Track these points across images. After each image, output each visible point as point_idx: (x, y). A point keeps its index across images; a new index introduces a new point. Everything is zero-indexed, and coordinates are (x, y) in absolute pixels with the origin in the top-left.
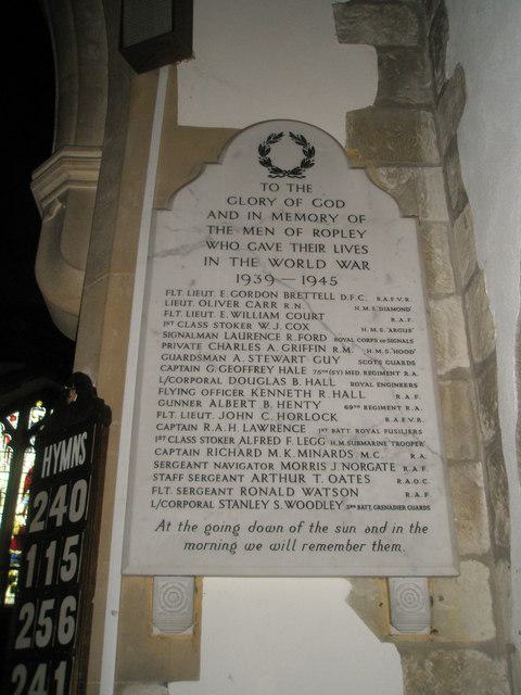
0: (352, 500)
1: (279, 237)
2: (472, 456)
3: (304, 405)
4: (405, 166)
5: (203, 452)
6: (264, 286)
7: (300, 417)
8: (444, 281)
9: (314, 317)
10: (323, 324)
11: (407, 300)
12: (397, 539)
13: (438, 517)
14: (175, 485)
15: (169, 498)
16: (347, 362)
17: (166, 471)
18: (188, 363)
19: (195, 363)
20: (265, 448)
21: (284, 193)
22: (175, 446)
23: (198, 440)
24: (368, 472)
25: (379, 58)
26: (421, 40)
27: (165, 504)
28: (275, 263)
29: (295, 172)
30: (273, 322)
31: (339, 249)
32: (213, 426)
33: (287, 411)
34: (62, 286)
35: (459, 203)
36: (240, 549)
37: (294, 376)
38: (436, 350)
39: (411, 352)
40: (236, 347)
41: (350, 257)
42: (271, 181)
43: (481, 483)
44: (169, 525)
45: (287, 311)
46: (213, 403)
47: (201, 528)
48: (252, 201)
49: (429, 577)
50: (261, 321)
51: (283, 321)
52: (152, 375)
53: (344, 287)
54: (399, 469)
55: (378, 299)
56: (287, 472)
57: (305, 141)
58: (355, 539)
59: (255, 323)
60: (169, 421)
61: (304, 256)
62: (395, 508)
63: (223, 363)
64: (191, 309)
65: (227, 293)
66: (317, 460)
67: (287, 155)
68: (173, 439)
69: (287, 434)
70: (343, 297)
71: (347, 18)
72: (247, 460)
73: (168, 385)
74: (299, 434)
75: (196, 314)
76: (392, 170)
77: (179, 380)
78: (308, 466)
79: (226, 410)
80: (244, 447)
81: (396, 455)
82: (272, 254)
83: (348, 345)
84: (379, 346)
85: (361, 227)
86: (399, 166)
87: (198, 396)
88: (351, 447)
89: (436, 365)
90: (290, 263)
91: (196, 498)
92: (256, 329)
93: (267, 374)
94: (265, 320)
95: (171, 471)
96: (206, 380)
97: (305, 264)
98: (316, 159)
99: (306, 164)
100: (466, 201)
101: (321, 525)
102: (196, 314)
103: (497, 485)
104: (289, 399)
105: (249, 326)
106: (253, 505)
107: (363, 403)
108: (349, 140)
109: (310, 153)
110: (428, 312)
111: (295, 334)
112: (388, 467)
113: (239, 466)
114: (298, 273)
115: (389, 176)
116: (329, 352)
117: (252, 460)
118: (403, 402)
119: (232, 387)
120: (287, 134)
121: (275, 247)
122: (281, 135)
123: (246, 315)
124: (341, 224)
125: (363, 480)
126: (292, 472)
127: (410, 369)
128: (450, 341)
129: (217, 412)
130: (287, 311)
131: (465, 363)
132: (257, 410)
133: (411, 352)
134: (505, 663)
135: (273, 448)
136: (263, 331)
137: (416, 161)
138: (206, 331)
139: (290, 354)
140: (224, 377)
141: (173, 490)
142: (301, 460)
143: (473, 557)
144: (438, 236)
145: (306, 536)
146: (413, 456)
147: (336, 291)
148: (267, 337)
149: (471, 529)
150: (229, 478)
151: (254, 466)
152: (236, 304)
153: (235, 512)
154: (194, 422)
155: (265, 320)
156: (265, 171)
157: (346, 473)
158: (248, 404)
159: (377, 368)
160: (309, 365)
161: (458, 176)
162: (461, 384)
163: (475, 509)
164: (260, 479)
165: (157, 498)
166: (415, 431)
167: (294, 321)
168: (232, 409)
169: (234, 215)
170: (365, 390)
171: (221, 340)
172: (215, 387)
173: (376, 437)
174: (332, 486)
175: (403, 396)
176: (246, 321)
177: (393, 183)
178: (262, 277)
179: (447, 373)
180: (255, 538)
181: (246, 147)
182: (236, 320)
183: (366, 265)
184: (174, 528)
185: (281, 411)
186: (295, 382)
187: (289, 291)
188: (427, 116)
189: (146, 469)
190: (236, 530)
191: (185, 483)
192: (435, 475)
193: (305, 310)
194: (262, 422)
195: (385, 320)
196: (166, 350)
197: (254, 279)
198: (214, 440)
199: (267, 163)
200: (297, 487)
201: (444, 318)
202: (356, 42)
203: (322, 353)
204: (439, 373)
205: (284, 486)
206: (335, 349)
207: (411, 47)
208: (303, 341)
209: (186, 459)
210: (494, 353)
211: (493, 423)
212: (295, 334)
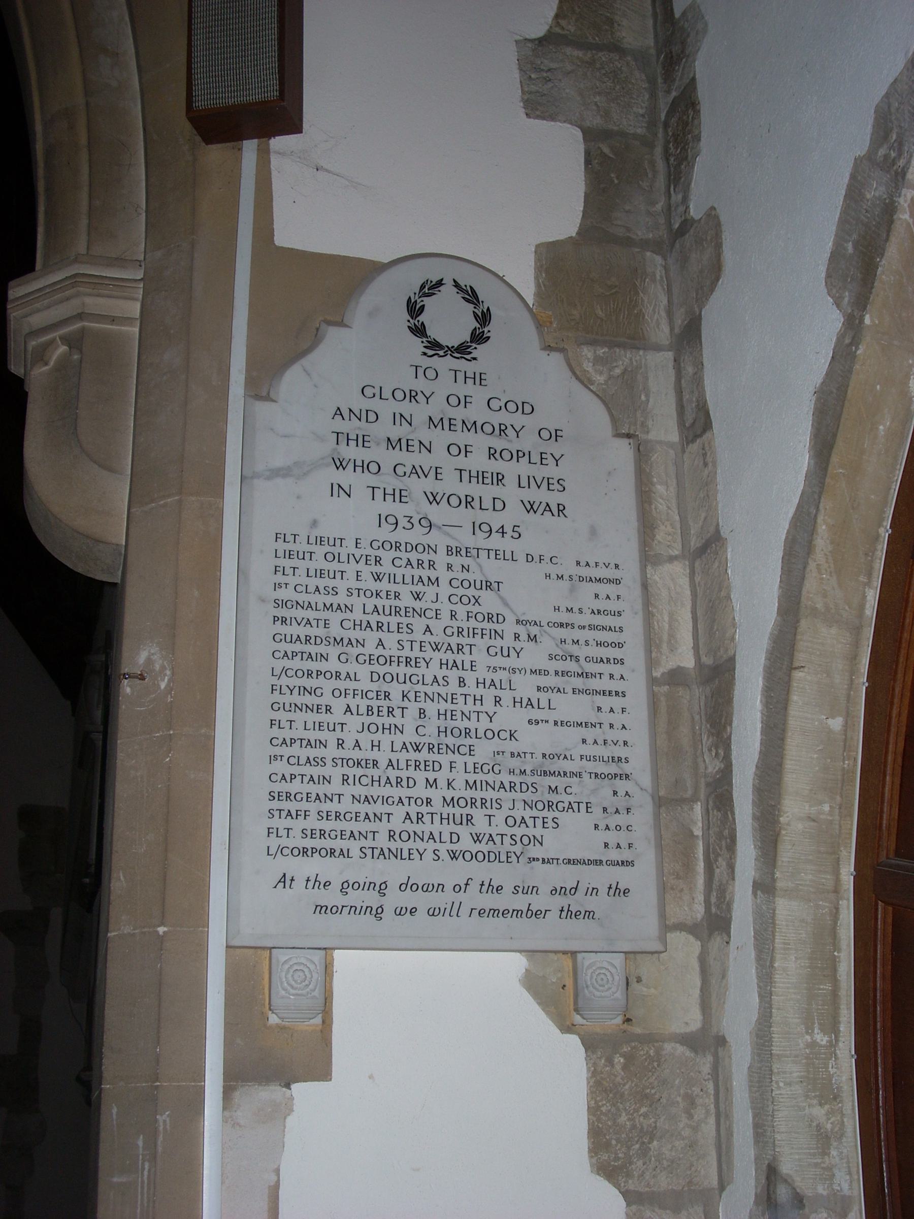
0: (535, 851)
1: (439, 457)
2: (690, 793)
3: (474, 716)
4: (619, 345)
5: (337, 780)
6: (416, 536)
7: (467, 732)
8: (667, 537)
9: (489, 586)
10: (501, 598)
11: (617, 566)
12: (591, 903)
13: (642, 878)
14: (299, 824)
15: (291, 843)
16: (533, 656)
17: (286, 805)
18: (312, 649)
19: (322, 649)
20: (420, 776)
21: (445, 386)
22: (296, 770)
23: (329, 762)
24: (557, 814)
25: (588, 153)
26: (652, 124)
27: (286, 851)
28: (433, 499)
29: (462, 350)
30: (430, 591)
31: (524, 483)
32: (349, 743)
33: (451, 724)
34: (81, 499)
35: (697, 424)
36: (388, 914)
37: (461, 673)
38: (651, 642)
39: (620, 645)
40: (379, 627)
41: (540, 496)
42: (425, 362)
43: (698, 832)
44: (292, 880)
45: (451, 575)
46: (348, 709)
47: (336, 886)
48: (399, 395)
49: (625, 953)
50: (415, 589)
51: (445, 590)
52: (261, 662)
53: (530, 543)
54: (597, 811)
55: (578, 563)
56: (450, 810)
57: (477, 299)
58: (538, 902)
59: (405, 591)
60: (287, 734)
61: (474, 489)
62: (590, 862)
63: (360, 650)
64: (313, 566)
65: (364, 543)
66: (490, 794)
67: (447, 316)
68: (292, 760)
69: (451, 757)
70: (529, 558)
71: (538, 70)
72: (396, 792)
73: (284, 681)
74: (467, 758)
75: (321, 573)
76: (601, 351)
77: (300, 674)
78: (478, 804)
79: (368, 720)
80: (393, 774)
81: (594, 791)
82: (429, 484)
83: (534, 630)
84: (577, 634)
85: (553, 448)
86: (611, 345)
87: (327, 699)
88: (535, 779)
89: (651, 663)
90: (454, 501)
91: (328, 843)
92: (407, 601)
93: (423, 670)
94: (419, 588)
95: (292, 806)
96: (338, 675)
97: (476, 503)
98: (493, 329)
99: (478, 338)
100: (707, 425)
101: (495, 884)
102: (321, 573)
103: (720, 836)
104: (453, 707)
105: (397, 596)
106: (405, 854)
107: (552, 716)
108: (538, 294)
109: (484, 318)
110: (645, 586)
111: (461, 610)
112: (583, 807)
113: (386, 800)
114: (465, 516)
115: (597, 360)
116: (508, 641)
117: (403, 792)
118: (606, 718)
119: (374, 687)
120: (448, 282)
121: (433, 472)
122: (440, 283)
123: (392, 579)
124: (529, 442)
125: (550, 824)
126: (457, 811)
127: (616, 670)
128: (670, 626)
129: (354, 722)
130: (451, 575)
131: (689, 662)
132: (410, 721)
133: (620, 645)
134: (710, 1058)
135: (431, 776)
136: (417, 605)
137: (636, 340)
138: (335, 600)
139: (454, 641)
140: (363, 671)
141: (296, 833)
142: (469, 794)
143: (680, 927)
144: (662, 465)
145: (474, 898)
146: (615, 793)
147: (519, 548)
148: (422, 613)
149: (682, 890)
150: (372, 816)
151: (406, 801)
152: (378, 561)
153: (381, 863)
154: (323, 735)
155: (419, 588)
156: (417, 344)
157: (527, 814)
158: (398, 712)
159: (572, 666)
160: (480, 657)
161: (698, 379)
162: (681, 691)
163: (688, 867)
164: (414, 819)
165: (274, 843)
166: (620, 759)
167: (460, 592)
168: (374, 718)
169: (372, 417)
170: (555, 697)
171: (358, 615)
172: (351, 685)
173: (568, 766)
174: (509, 831)
175: (606, 709)
176: (393, 588)
177: (601, 373)
178: (415, 521)
179: (663, 674)
180: (408, 899)
181: (385, 298)
182: (378, 586)
183: (561, 509)
184: (299, 884)
185: (442, 723)
186: (462, 682)
187: (454, 544)
188: (655, 262)
189: (257, 800)
190: (382, 889)
191: (312, 823)
192: (642, 819)
193: (475, 575)
194: (416, 739)
195: (586, 595)
196: (279, 628)
197: (403, 522)
198: (351, 763)
199: (419, 331)
200: (464, 831)
201: (664, 593)
202: (552, 118)
203: (498, 642)
204: (654, 674)
205: (446, 829)
206: (517, 637)
207: (635, 136)
208: (472, 623)
209: (314, 789)
210: (732, 660)
211: (721, 752)
212: (461, 610)
